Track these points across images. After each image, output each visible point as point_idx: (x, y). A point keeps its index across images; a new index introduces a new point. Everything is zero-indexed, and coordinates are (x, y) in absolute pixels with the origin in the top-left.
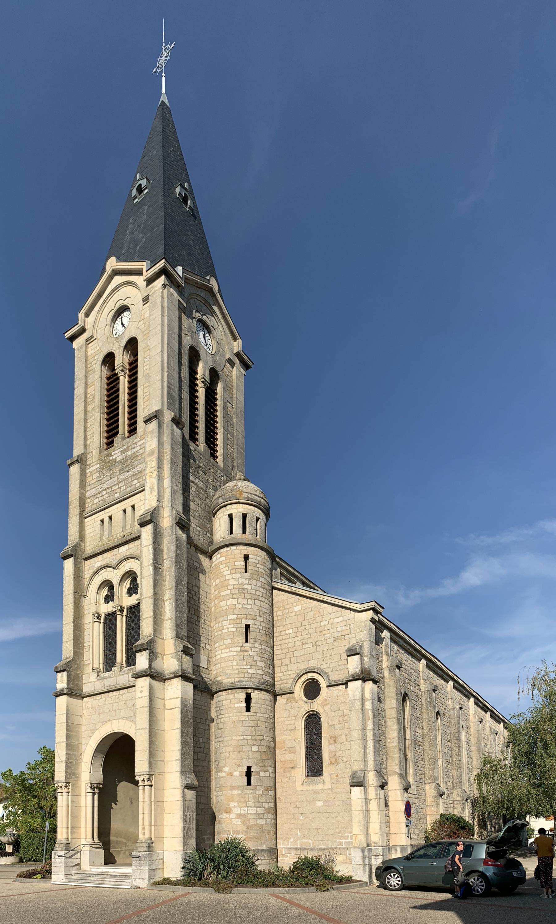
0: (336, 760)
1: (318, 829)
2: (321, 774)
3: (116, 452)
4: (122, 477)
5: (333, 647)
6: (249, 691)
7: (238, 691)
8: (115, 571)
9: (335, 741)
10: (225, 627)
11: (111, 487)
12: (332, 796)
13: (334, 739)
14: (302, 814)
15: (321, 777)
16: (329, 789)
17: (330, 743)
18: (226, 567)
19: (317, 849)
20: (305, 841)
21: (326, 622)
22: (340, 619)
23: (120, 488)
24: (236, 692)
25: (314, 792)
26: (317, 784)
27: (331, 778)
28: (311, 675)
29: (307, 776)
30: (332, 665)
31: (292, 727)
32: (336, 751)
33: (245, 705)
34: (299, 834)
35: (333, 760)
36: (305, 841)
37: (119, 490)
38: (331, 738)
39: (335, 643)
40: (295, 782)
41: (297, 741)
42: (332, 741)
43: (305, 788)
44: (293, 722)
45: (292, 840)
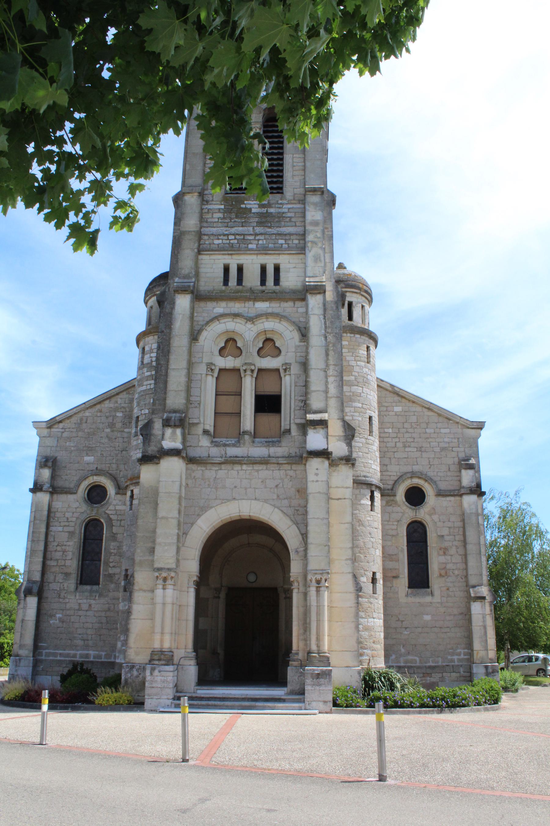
0: (446, 572)
1: (425, 645)
2: (428, 587)
3: (251, 202)
4: (259, 230)
5: (440, 456)
6: (373, 489)
7: (364, 487)
8: (249, 325)
9: (444, 553)
10: (348, 414)
11: (244, 235)
12: (442, 610)
13: (445, 551)
14: (406, 628)
15: (428, 590)
16: (438, 603)
17: (439, 555)
18: (349, 352)
19: (425, 667)
20: (410, 657)
21: (432, 431)
22: (447, 431)
23: (258, 240)
24: (362, 488)
25: (421, 605)
26: (423, 598)
27: (441, 591)
28: (416, 481)
29: (409, 587)
30: (439, 474)
31: (394, 533)
32: (446, 564)
33: (369, 503)
34: (403, 650)
35: (443, 572)
36: (410, 657)
37: (256, 242)
38: (440, 549)
39: (442, 453)
40: (397, 593)
41: (400, 548)
42: (441, 552)
43: (411, 599)
44: (395, 527)
45: (393, 657)
